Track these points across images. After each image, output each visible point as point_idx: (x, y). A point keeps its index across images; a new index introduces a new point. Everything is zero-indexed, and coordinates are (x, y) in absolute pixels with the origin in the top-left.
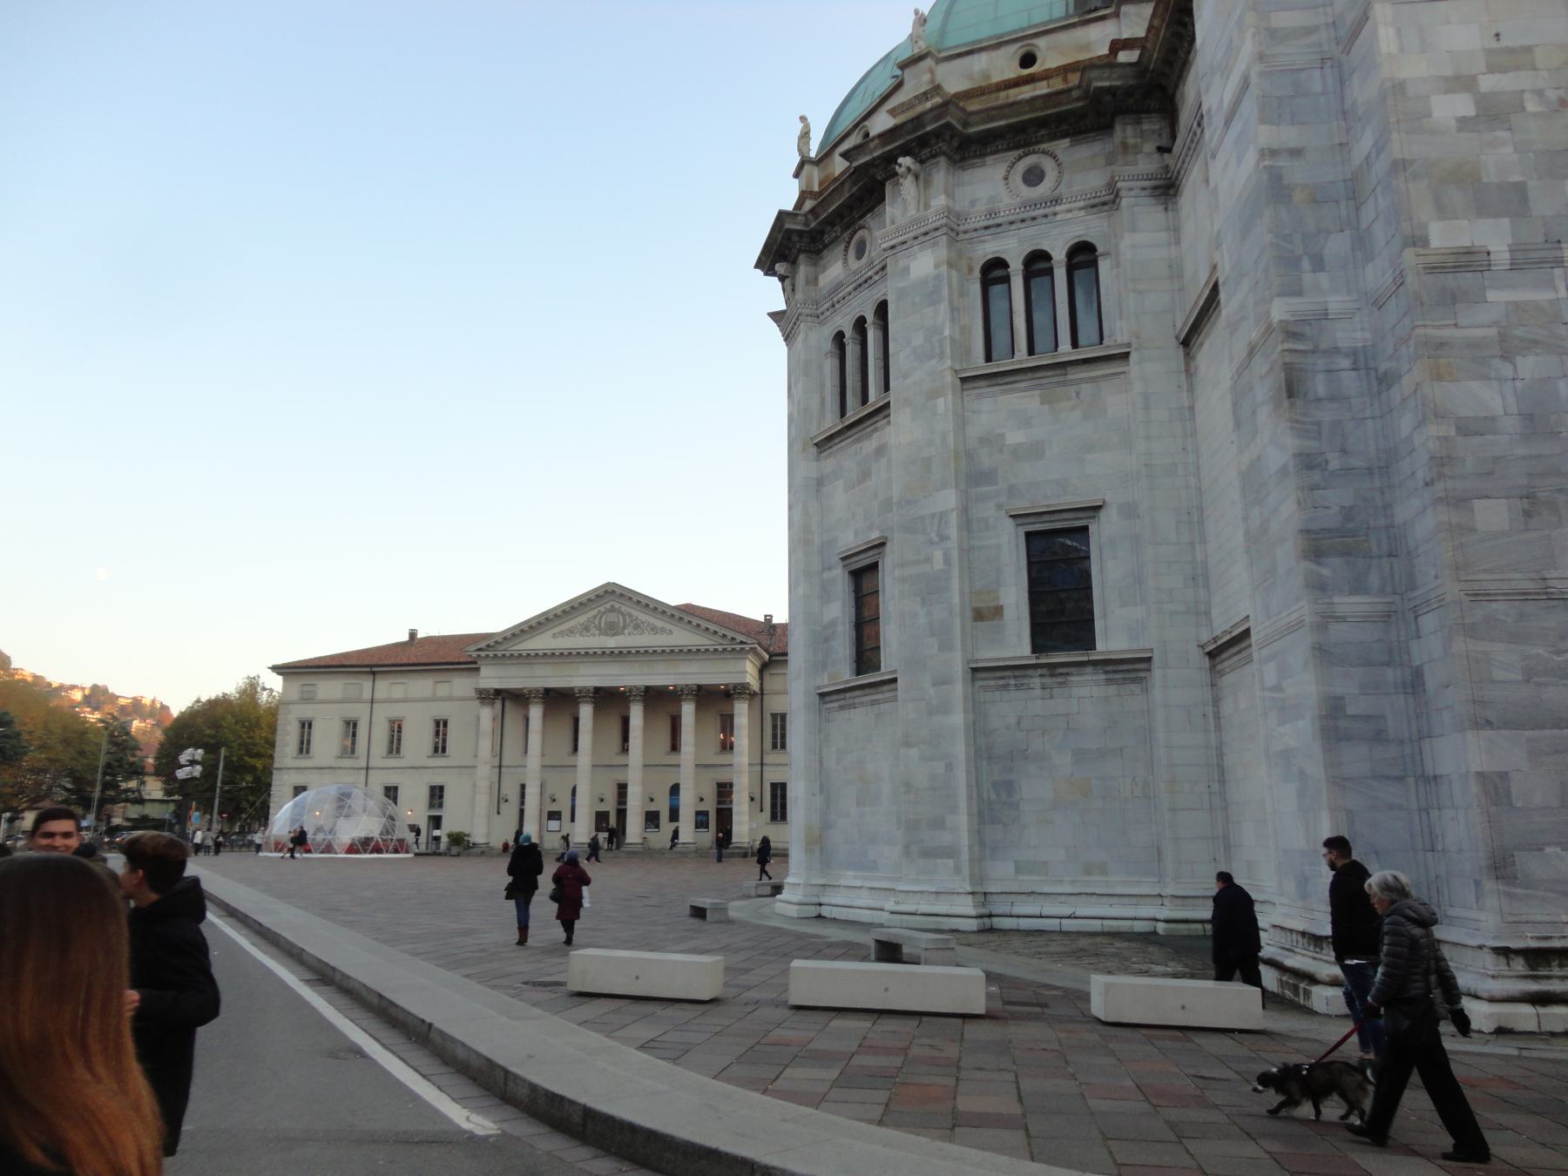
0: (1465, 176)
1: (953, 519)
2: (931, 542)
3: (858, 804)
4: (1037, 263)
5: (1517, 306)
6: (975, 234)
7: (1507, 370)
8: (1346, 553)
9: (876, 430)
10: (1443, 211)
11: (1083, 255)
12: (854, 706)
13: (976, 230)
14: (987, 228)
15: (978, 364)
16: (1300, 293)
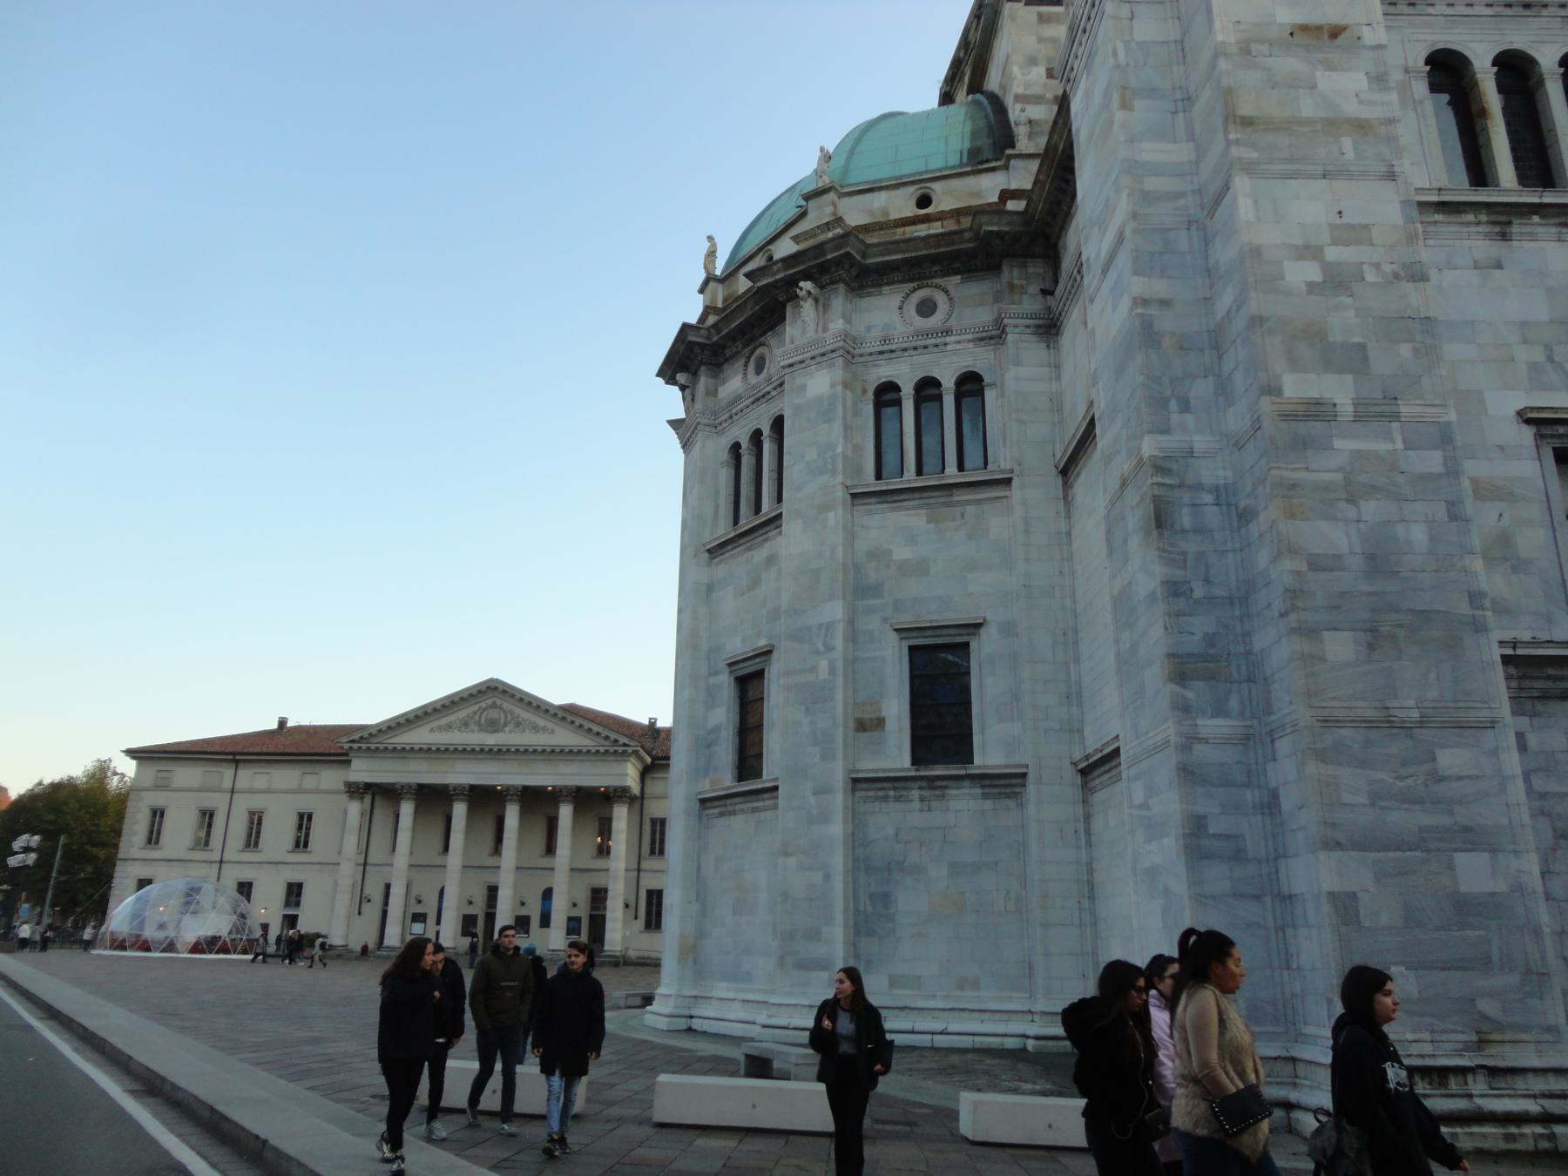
0: (1314, 335)
1: (840, 630)
2: (817, 652)
3: (735, 913)
4: (927, 388)
5: (1359, 455)
6: (869, 358)
7: (1351, 512)
8: (1211, 677)
9: (767, 540)
10: (1295, 365)
11: (971, 385)
12: (734, 813)
13: (871, 354)
14: (881, 353)
15: (868, 481)
16: (1167, 431)
